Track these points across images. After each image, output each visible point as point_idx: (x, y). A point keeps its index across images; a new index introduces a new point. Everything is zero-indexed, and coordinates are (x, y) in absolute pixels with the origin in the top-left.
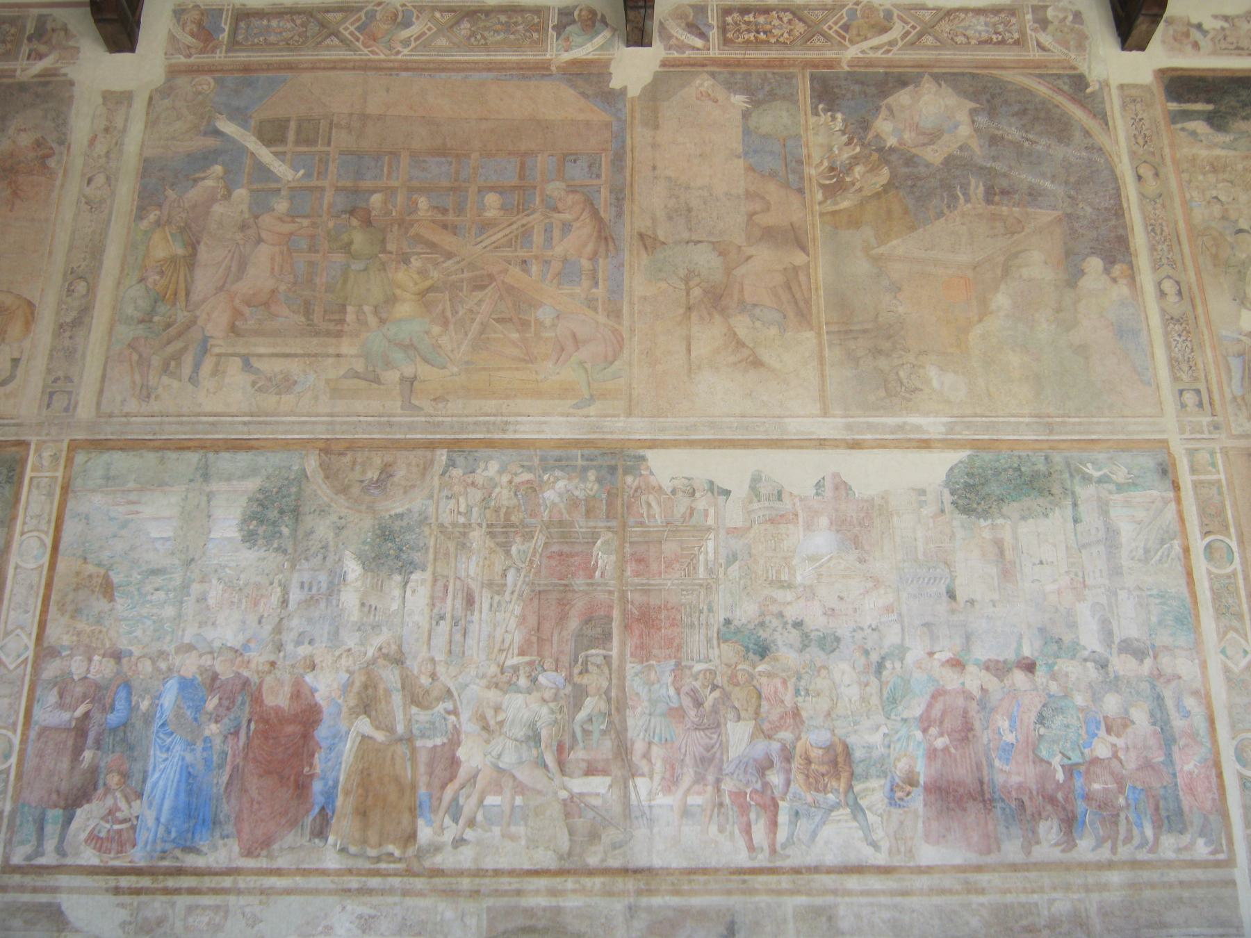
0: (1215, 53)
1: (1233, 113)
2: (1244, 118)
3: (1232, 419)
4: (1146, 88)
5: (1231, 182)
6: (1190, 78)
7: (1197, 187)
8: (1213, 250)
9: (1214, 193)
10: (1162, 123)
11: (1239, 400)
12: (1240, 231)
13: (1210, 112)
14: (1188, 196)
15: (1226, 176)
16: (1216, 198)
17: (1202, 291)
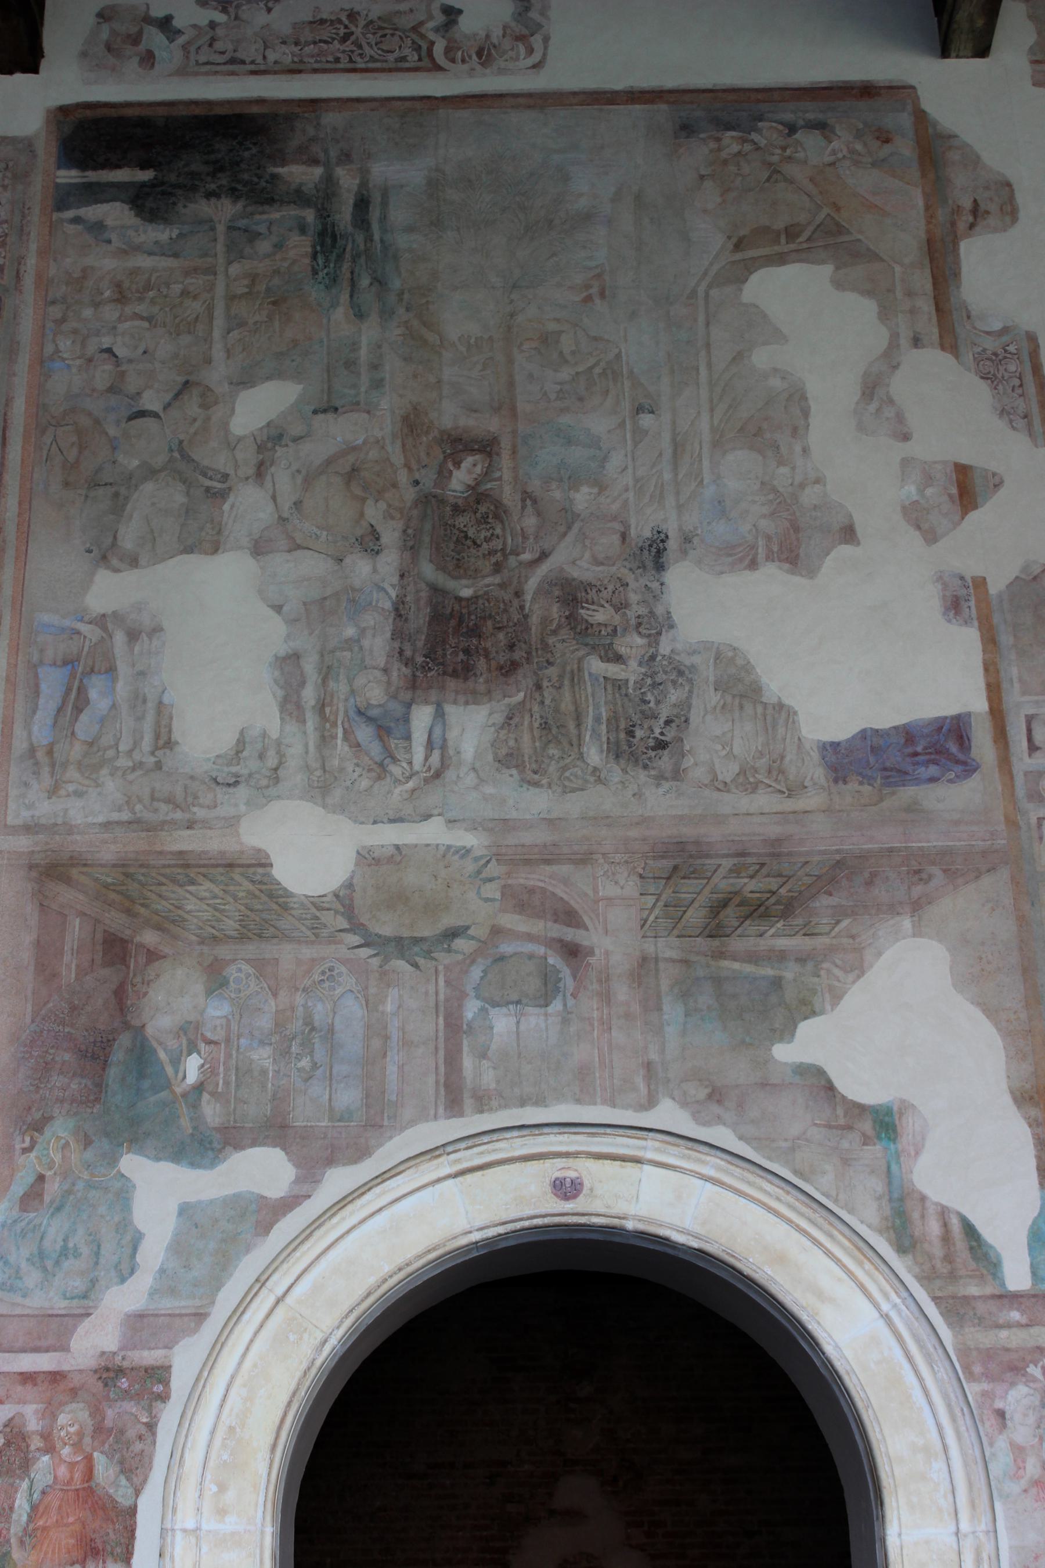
0: (182, 72)
1: (191, 187)
2: (209, 195)
3: (13, 792)
4: (27, 145)
5: (149, 319)
6: (121, 121)
7: (75, 332)
8: (72, 455)
9: (106, 342)
10: (37, 210)
11: (40, 755)
12: (142, 414)
13: (143, 185)
14: (49, 349)
15: (141, 309)
16: (109, 351)
17: (25, 535)
